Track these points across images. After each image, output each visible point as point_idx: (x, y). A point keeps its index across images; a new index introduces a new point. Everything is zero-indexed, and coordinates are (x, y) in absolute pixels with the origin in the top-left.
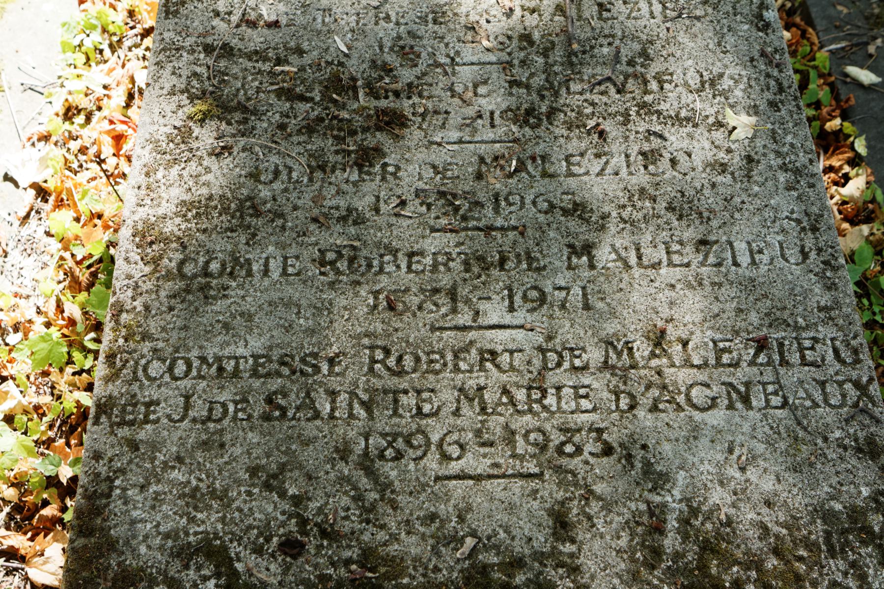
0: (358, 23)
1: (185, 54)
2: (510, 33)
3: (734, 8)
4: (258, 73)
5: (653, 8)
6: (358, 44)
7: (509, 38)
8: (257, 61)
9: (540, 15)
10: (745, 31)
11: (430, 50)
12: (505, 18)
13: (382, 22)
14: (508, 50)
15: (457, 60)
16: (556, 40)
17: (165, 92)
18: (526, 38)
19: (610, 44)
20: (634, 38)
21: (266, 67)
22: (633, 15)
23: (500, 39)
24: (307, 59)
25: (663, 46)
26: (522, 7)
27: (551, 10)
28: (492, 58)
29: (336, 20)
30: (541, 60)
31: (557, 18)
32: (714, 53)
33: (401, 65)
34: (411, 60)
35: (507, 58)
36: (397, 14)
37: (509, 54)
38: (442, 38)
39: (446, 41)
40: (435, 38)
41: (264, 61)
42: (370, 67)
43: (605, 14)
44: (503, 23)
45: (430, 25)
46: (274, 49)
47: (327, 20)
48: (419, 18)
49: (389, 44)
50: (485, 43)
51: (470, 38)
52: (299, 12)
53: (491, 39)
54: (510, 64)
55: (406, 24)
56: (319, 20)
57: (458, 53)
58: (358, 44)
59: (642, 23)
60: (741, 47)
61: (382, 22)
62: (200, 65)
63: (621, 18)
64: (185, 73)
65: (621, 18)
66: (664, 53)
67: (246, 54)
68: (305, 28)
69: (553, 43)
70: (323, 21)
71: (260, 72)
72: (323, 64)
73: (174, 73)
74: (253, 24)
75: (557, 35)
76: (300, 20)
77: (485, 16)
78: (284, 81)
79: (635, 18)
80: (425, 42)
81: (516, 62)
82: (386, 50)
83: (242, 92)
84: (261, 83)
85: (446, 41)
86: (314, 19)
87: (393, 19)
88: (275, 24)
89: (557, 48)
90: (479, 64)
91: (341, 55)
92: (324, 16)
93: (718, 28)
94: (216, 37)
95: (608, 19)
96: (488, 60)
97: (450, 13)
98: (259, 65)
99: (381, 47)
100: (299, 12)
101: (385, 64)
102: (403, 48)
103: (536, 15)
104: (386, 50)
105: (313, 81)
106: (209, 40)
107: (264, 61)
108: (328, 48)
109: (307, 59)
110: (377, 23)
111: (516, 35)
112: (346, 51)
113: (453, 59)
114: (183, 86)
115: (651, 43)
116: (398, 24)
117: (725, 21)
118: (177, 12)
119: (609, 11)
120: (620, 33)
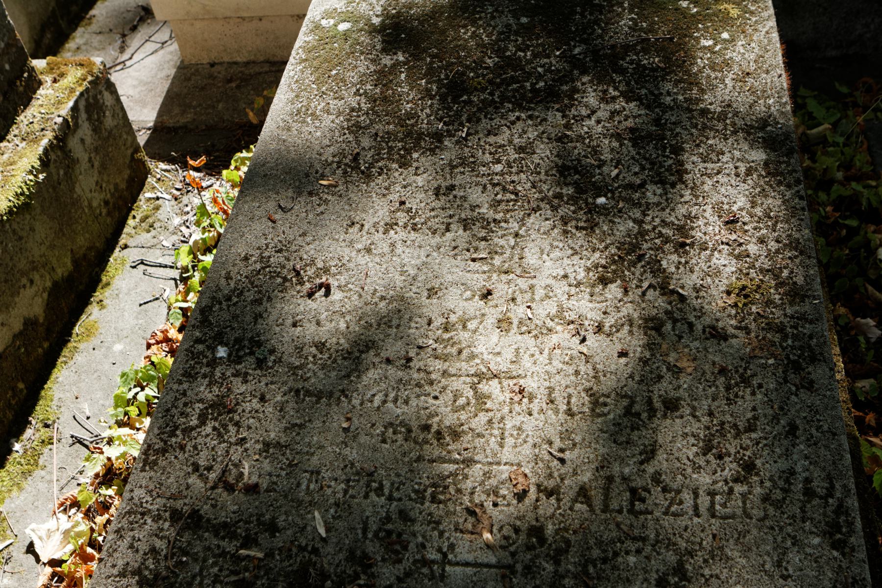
0: (346, 492)
1: (149, 521)
2: (518, 523)
3: (803, 510)
4: (220, 556)
5: (699, 501)
6: (341, 524)
7: (517, 530)
8: (223, 538)
9: (559, 500)
10: (814, 547)
11: (420, 539)
12: (515, 502)
13: (373, 495)
14: (512, 549)
15: (450, 557)
16: (573, 538)
17: (115, 571)
18: (537, 531)
19: (638, 551)
20: (670, 544)
21: (230, 546)
22: (673, 509)
23: (505, 532)
24: (279, 541)
25: (705, 561)
26: (538, 486)
27: (572, 494)
28: (493, 560)
29: (322, 488)
30: (549, 567)
31: (578, 506)
32: (771, 577)
33: (384, 560)
34: (397, 552)
35: (510, 561)
36: (392, 484)
37: (513, 554)
38: (438, 523)
39: (441, 527)
40: (430, 523)
41: (231, 539)
42: (346, 560)
43: (638, 506)
44: (511, 508)
45: (427, 504)
46: (247, 522)
47: (312, 486)
48: (417, 492)
49: (375, 527)
50: (487, 536)
51: (469, 527)
52: (283, 473)
53: (495, 530)
54: (511, 568)
55: (400, 499)
56: (304, 487)
57: (452, 547)
58: (341, 524)
59: (683, 522)
60: (808, 571)
61: (373, 495)
62: (161, 538)
63: (657, 514)
64: (143, 547)
65: (657, 514)
66: (707, 572)
67: (214, 526)
68: (286, 497)
69: (568, 542)
70: (308, 487)
71: (224, 554)
72: (294, 550)
73: (131, 546)
74: (230, 488)
75: (575, 532)
76: (284, 484)
77: (492, 498)
78: (246, 569)
79: (675, 515)
80: (417, 528)
81: (519, 567)
82: (370, 536)
83: (198, 579)
84: (220, 570)
85: (441, 527)
86: (299, 485)
87: (386, 491)
88: (252, 489)
89: (573, 550)
90: (476, 565)
91: (318, 539)
92: (310, 481)
93: (779, 539)
94: (187, 501)
95: (641, 513)
96: (486, 560)
97: (452, 490)
98: (224, 544)
99: (365, 530)
100: (283, 473)
101: (365, 555)
102: (389, 533)
103: (553, 500)
104: (370, 536)
105: (279, 574)
106: (179, 504)
107: (231, 539)
108: (305, 527)
109: (279, 541)
110: (366, 496)
111: (524, 527)
112: (324, 535)
113: (445, 555)
114: (136, 565)
115: (691, 554)
116: (390, 498)
117: (789, 529)
118: (155, 463)
119: (643, 500)
120: (652, 536)
